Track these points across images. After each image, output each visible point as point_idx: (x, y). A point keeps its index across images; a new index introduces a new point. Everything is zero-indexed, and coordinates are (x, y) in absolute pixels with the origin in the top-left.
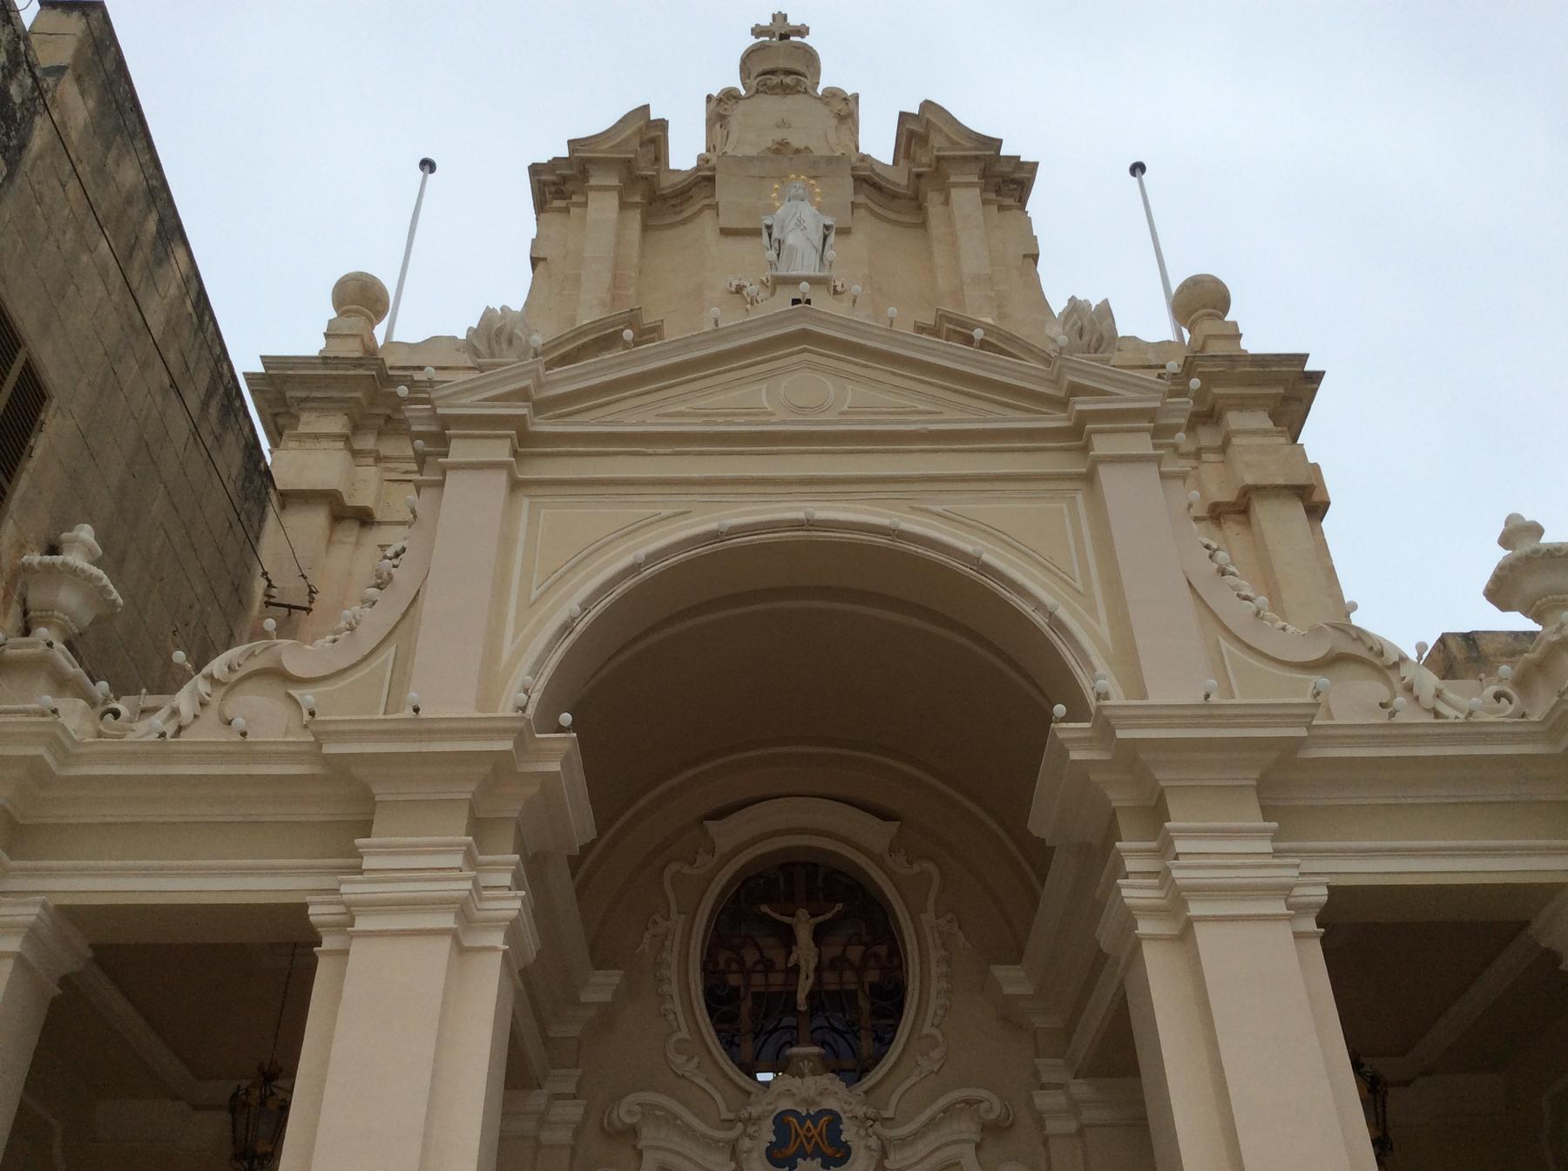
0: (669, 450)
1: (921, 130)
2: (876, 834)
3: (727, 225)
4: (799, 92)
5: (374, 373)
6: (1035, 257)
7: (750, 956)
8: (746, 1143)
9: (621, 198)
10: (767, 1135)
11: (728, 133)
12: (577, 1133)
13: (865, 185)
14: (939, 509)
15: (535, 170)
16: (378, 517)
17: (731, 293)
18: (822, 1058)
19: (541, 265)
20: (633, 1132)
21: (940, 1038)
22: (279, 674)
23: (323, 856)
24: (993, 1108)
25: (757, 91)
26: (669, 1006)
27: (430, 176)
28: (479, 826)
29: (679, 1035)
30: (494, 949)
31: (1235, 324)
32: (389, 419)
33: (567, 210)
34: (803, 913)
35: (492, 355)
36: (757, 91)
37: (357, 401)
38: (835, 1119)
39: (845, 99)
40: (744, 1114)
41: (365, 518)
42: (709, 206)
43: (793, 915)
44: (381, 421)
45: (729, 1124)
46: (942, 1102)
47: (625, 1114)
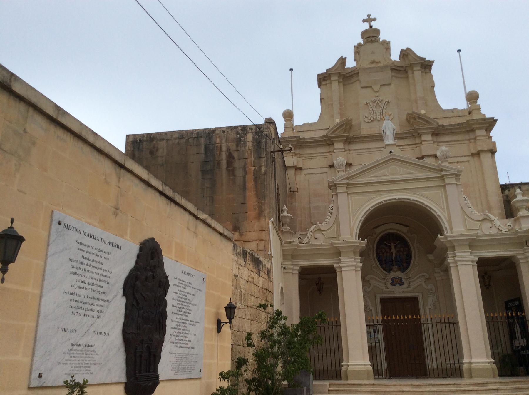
1: (407, 54)
2: (404, 229)
4: (376, 42)
6: (434, 87)
7: (383, 251)
11: (360, 57)
14: (418, 193)
15: (318, 75)
16: (303, 168)
17: (365, 105)
22: (320, 230)
24: (428, 276)
25: (366, 43)
27: (292, 72)
28: (355, 253)
29: (373, 265)
30: (360, 270)
32: (300, 146)
33: (326, 84)
34: (392, 244)
35: (340, 168)
36: (366, 43)
37: (295, 144)
38: (401, 279)
39: (387, 44)
41: (301, 169)
42: (358, 80)
43: (390, 244)
44: (299, 146)
45: (384, 279)
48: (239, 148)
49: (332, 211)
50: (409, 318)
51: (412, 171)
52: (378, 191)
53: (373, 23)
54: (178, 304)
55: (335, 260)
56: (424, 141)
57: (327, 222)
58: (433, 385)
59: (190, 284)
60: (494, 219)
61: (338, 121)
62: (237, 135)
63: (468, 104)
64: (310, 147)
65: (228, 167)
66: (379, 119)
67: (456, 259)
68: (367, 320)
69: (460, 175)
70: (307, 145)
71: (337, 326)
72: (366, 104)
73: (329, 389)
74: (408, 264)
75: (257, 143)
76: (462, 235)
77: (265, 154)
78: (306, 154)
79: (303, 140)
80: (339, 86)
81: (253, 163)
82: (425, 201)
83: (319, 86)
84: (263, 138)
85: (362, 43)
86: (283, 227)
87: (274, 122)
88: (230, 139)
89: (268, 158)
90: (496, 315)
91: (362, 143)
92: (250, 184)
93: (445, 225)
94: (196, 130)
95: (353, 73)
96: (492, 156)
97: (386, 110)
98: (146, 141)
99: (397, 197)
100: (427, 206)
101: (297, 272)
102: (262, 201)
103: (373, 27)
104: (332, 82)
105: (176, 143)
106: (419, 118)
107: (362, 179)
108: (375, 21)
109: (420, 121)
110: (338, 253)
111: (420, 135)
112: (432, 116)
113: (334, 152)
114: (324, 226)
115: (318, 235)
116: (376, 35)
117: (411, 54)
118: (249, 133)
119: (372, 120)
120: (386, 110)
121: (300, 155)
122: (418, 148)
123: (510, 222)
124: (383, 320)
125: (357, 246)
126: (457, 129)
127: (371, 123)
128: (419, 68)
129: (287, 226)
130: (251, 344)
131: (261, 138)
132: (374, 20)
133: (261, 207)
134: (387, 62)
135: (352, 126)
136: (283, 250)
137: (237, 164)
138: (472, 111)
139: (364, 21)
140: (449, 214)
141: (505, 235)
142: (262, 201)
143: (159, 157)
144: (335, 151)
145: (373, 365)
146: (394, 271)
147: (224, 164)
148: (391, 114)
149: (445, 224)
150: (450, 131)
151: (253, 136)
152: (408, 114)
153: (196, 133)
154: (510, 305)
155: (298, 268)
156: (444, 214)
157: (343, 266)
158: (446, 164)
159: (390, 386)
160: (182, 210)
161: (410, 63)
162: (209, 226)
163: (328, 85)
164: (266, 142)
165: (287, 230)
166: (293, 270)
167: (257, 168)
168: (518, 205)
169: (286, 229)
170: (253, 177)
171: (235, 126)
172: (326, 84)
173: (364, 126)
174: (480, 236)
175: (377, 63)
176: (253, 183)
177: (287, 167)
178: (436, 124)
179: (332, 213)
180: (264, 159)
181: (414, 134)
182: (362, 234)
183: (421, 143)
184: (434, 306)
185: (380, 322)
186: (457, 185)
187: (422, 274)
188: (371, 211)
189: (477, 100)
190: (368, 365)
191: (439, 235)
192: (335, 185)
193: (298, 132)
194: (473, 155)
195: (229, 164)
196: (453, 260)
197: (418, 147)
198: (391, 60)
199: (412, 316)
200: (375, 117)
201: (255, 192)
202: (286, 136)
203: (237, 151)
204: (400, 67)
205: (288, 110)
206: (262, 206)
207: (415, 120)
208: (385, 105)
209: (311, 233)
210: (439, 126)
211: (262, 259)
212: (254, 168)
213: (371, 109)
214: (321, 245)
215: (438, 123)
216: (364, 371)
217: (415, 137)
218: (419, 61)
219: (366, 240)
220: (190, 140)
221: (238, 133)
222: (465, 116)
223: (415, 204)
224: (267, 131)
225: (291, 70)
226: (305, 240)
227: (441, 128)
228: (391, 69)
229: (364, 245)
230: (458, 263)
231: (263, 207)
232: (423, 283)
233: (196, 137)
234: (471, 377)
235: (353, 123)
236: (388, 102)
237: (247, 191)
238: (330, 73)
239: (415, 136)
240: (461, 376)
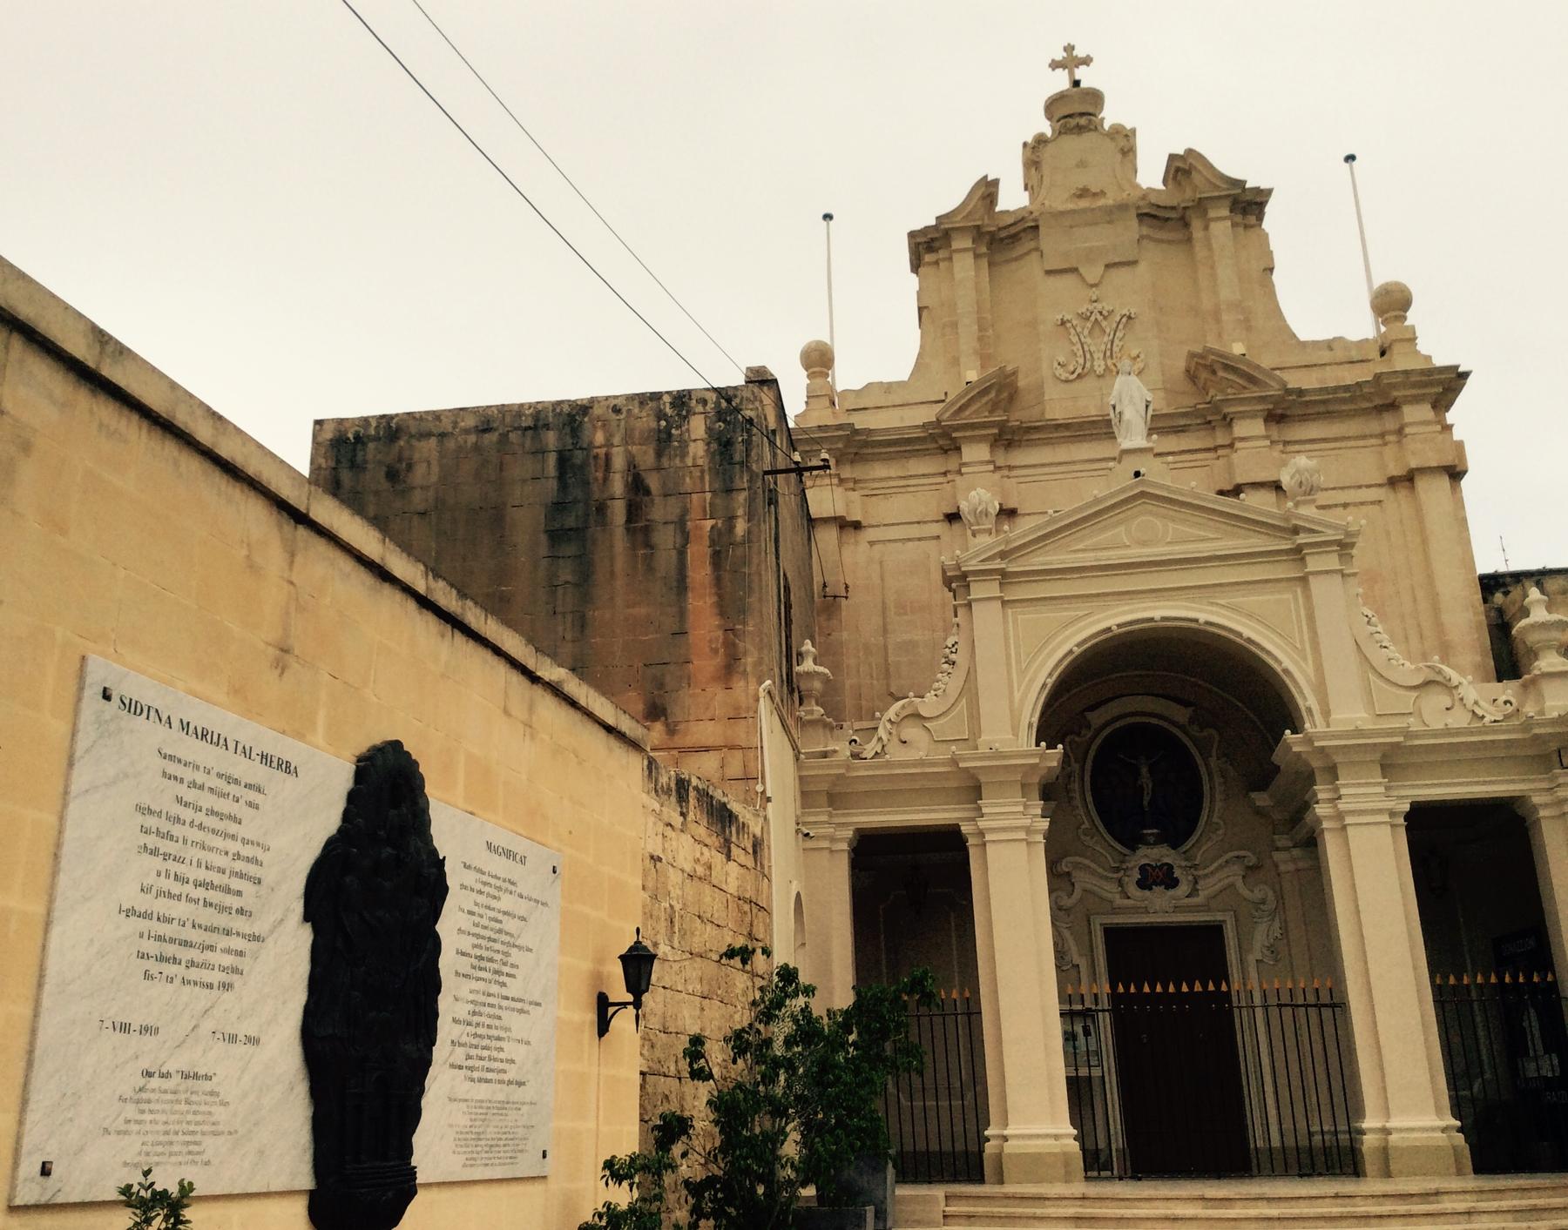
2: (1181, 714)
3: (1048, 268)
4: (1091, 130)
6: (1271, 270)
8: (1126, 879)
9: (975, 254)
13: (1145, 218)
15: (912, 235)
21: (1222, 823)
22: (917, 716)
23: (959, 804)
24: (1253, 860)
26: (1077, 812)
27: (831, 223)
28: (1025, 787)
31: (1413, 328)
32: (856, 454)
33: (937, 263)
35: (978, 524)
36: (1060, 133)
37: (838, 449)
38: (1170, 867)
39: (1127, 136)
41: (857, 526)
42: (1037, 249)
45: (1117, 870)
48: (665, 462)
49: (953, 657)
50: (1196, 990)
51: (1202, 533)
52: (1098, 595)
53: (1081, 73)
54: (475, 946)
55: (964, 809)
56: (1242, 439)
57: (939, 692)
58: (1269, 1200)
59: (513, 884)
61: (972, 375)
62: (659, 420)
63: (1377, 322)
64: (888, 458)
65: (629, 520)
66: (1100, 370)
67: (1342, 806)
68: (1064, 997)
69: (1352, 545)
70: (876, 450)
71: (969, 1014)
72: (1059, 323)
73: (944, 1211)
75: (722, 446)
76: (1359, 733)
78: (874, 480)
80: (977, 269)
81: (708, 509)
82: (1244, 625)
83: (916, 266)
85: (1049, 133)
86: (802, 708)
87: (776, 381)
88: (637, 434)
89: (756, 493)
90: (1465, 982)
91: (1048, 444)
92: (700, 572)
93: (1306, 699)
94: (530, 405)
97: (1121, 343)
98: (377, 439)
100: (1249, 640)
101: (845, 846)
102: (738, 627)
103: (1083, 85)
104: (956, 257)
105: (469, 444)
106: (1227, 367)
107: (1049, 558)
108: (1088, 65)
109: (1231, 377)
110: (973, 790)
111: (1228, 421)
112: (1266, 362)
113: (962, 474)
114: (928, 705)
115: (911, 732)
117: (1200, 168)
118: (695, 414)
119: (1079, 375)
120: (1121, 343)
121: (856, 481)
122: (1221, 462)
123: (1508, 690)
124: (1114, 996)
126: (1343, 401)
127: (1076, 385)
128: (1225, 212)
129: (813, 702)
130: (702, 1069)
132: (1087, 61)
133: (734, 645)
134: (1125, 195)
136: (801, 778)
137: (661, 511)
138: (1390, 346)
139: (1055, 65)
140: (1319, 668)
141: (1495, 732)
142: (738, 627)
143: (414, 488)
144: (964, 470)
145: (1080, 1138)
146: (1147, 844)
147: (618, 511)
149: (1305, 699)
150: (1322, 409)
152: (1192, 355)
153: (531, 414)
155: (849, 833)
156: (1304, 665)
157: (991, 829)
158: (1308, 511)
159: (1136, 1203)
160: (488, 655)
161: (1198, 196)
162: (573, 703)
163: (941, 264)
164: (748, 443)
165: (816, 716)
166: (833, 839)
167: (720, 522)
168: (1533, 638)
169: (811, 712)
170: (709, 551)
171: (651, 393)
172: (937, 263)
173: (1053, 392)
174: (1417, 735)
175: (1095, 195)
176: (708, 569)
177: (816, 519)
178: (1277, 387)
179: (954, 663)
180: (742, 497)
181: (1209, 418)
182: (1050, 728)
183: (1231, 446)
185: (1105, 1003)
187: (1236, 853)
189: (1406, 311)
190: (1067, 1136)
191: (1288, 732)
192: (964, 576)
193: (847, 410)
194: (1392, 482)
195: (633, 511)
196: (1331, 810)
197: (1223, 456)
198: (1138, 186)
199: (1205, 986)
200: (1088, 365)
201: (715, 599)
202: (813, 423)
203: (659, 469)
204: (1165, 208)
205: (819, 343)
207: (1214, 372)
208: (1121, 326)
209: (889, 726)
210: (1289, 392)
211: (735, 807)
212: (712, 522)
213: (1075, 339)
214: (921, 763)
215: (1284, 384)
216: (1055, 1155)
217: (1214, 428)
219: (1060, 746)
220: (513, 437)
221: (660, 415)
222: (1369, 361)
223: (1213, 634)
224: (751, 406)
226: (870, 748)
227: (1294, 397)
229: (1055, 764)
230: (1348, 820)
231: (741, 645)
232: (1239, 884)
233: (529, 428)
235: (1021, 383)
236: (1130, 318)
237: (690, 595)
238: (947, 226)
239: (1213, 424)
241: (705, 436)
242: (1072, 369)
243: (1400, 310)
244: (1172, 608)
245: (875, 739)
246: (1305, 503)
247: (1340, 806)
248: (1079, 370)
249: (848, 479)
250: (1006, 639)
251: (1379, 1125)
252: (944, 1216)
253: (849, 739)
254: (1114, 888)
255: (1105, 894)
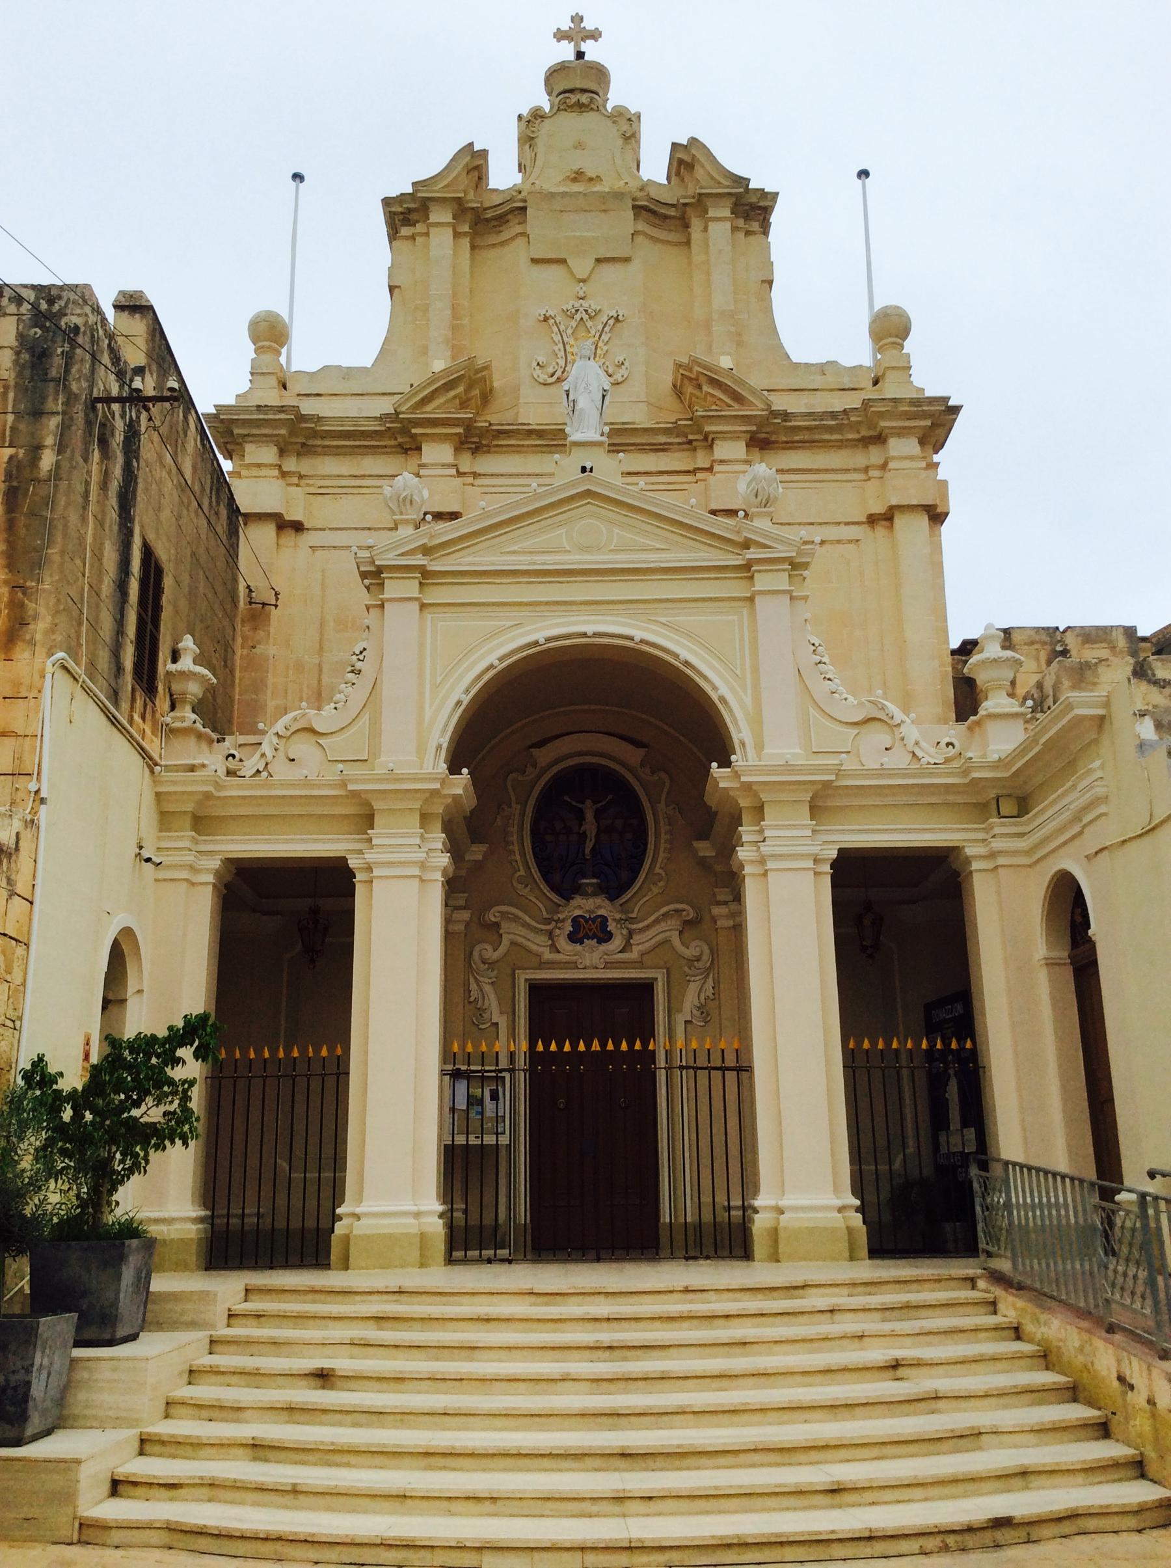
0: (509, 581)
1: (689, 160)
2: (633, 756)
3: (536, 257)
4: (592, 109)
5: (293, 417)
6: (770, 283)
8: (557, 932)
10: (569, 928)
12: (467, 925)
14: (663, 620)
15: (387, 202)
16: (307, 525)
17: (540, 321)
18: (599, 886)
19: (396, 291)
20: (497, 925)
21: (663, 874)
22: (311, 731)
26: (513, 857)
28: (425, 818)
32: (304, 445)
33: (413, 238)
34: (589, 803)
35: (401, 514)
36: (559, 109)
38: (604, 919)
39: (629, 120)
40: (556, 918)
41: (298, 527)
45: (547, 921)
46: (665, 909)
47: (492, 916)
49: (359, 665)
50: (593, 1049)
53: (587, 47)
56: (722, 462)
60: (902, 721)
61: (439, 365)
64: (337, 452)
69: (805, 566)
71: (338, 1075)
72: (542, 318)
73: (229, 1310)
74: (635, 872)
76: (788, 768)
77: (60, 402)
78: (324, 477)
79: (313, 425)
81: (8, 433)
84: (59, 339)
85: (547, 108)
86: (172, 714)
87: (152, 306)
89: (71, 419)
90: (895, 1045)
91: (518, 452)
93: (740, 730)
95: (506, 208)
96: (931, 527)
97: (605, 348)
99: (590, 629)
100: (687, 663)
101: (211, 878)
102: (29, 584)
103: (587, 58)
104: (432, 230)
106: (714, 382)
111: (708, 442)
112: (757, 380)
114: (323, 719)
115: (302, 748)
116: (592, 86)
120: (605, 348)
121: (301, 477)
122: (701, 485)
123: (954, 732)
124: (533, 1056)
125: (434, 793)
128: (726, 213)
129: (188, 708)
131: (54, 342)
132: (595, 35)
133: (22, 605)
134: (622, 183)
135: (491, 390)
136: (158, 794)
138: (884, 374)
139: (560, 36)
141: (931, 775)
146: (585, 895)
148: (623, 364)
150: (806, 436)
151: (20, 327)
154: (942, 1015)
155: (215, 863)
161: (698, 191)
164: (69, 358)
166: (192, 869)
167: (21, 451)
168: (981, 678)
169: (183, 719)
172: (413, 238)
175: (591, 179)
177: (247, 516)
178: (761, 406)
180: (54, 422)
181: (691, 437)
184: (702, 1013)
185: (521, 1062)
186: (791, 598)
187: (672, 907)
188: (499, 673)
189: (905, 338)
191: (715, 765)
193: (298, 395)
194: (872, 520)
196: (755, 854)
197: (701, 480)
199: (603, 1045)
202: (253, 402)
206: (26, 601)
207: (699, 387)
208: (607, 329)
209: (275, 740)
210: (774, 414)
212: (11, 451)
213: (557, 338)
214: (306, 783)
217: (695, 449)
218: (728, 187)
219: (465, 771)
222: (861, 389)
224: (78, 311)
225: (298, 180)
227: (779, 421)
228: (634, 207)
230: (770, 865)
231: (30, 605)
232: (676, 941)
234: (775, 1258)
236: (617, 320)
239: (695, 443)
240: (746, 1254)
241: (15, 344)
242: (551, 370)
243: (897, 336)
244: (614, 623)
245: (258, 755)
246: (760, 515)
247: (762, 849)
248: (558, 374)
249: (294, 473)
250: (421, 645)
251: (772, 1203)
252: (230, 1316)
253: (227, 753)
254: (543, 940)
255: (534, 947)
